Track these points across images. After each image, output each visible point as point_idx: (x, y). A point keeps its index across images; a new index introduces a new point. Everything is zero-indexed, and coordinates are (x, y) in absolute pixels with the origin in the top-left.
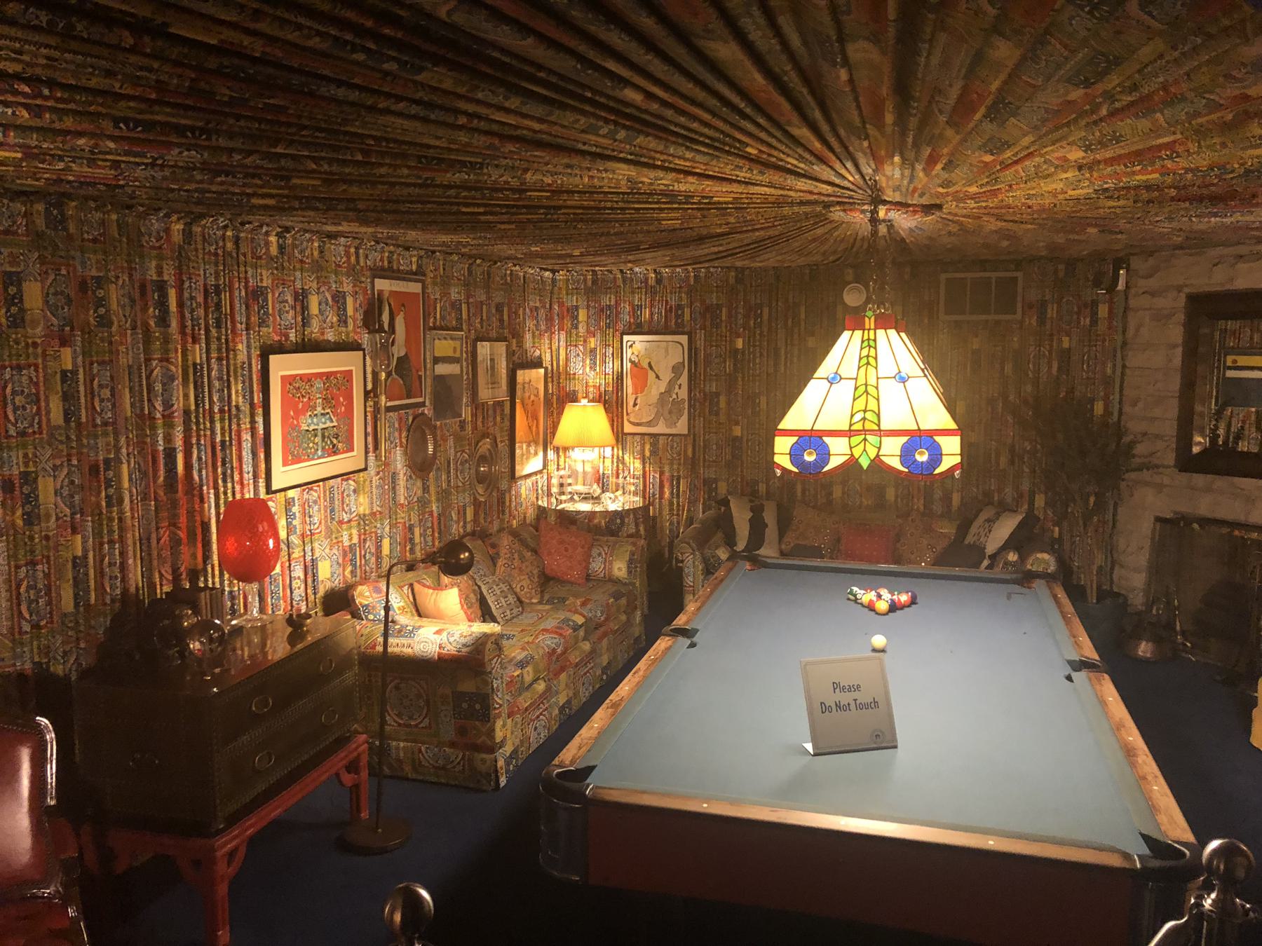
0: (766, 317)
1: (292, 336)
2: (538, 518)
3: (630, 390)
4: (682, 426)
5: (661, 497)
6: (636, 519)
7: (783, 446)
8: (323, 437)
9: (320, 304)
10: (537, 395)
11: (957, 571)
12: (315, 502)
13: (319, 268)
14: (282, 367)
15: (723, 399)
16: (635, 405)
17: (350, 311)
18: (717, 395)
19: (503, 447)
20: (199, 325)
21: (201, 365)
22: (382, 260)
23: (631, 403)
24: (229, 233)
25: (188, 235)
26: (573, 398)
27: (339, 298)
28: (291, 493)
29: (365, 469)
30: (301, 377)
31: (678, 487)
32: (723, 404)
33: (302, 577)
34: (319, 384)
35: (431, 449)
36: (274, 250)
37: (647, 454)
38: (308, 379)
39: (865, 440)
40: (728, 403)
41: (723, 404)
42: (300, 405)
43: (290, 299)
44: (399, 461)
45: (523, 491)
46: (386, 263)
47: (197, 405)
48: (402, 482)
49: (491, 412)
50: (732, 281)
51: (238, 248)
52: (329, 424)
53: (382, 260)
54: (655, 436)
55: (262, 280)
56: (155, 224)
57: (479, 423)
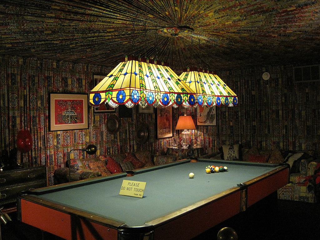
0: (239, 85)
1: (61, 89)
2: (167, 151)
3: (199, 111)
4: (214, 123)
5: (209, 147)
6: (198, 152)
7: (92, 96)
8: (71, 118)
9: (72, 81)
10: (169, 113)
11: (258, 163)
12: (69, 136)
13: (73, 72)
14: (54, 98)
15: (227, 113)
16: (200, 116)
17: (84, 83)
18: (225, 112)
19: (152, 128)
20: (26, 85)
21: (26, 95)
22: (98, 70)
23: (199, 115)
24: (39, 62)
25: (24, 63)
26: (182, 114)
27: (79, 81)
28: (59, 133)
29: (88, 129)
30: (63, 100)
31: (214, 143)
32: (227, 115)
33: (62, 157)
34: (69, 103)
35: (117, 126)
36: (55, 66)
37: (205, 132)
38: (66, 101)
39: (109, 93)
40: (229, 115)
41: (227, 115)
42: (62, 108)
43: (60, 80)
44: (104, 128)
45: (162, 143)
46: (99, 71)
47: (24, 106)
48: (105, 134)
49: (146, 117)
50: (228, 74)
51: (42, 66)
52: (73, 114)
53: (98, 70)
54: (207, 126)
55: (50, 75)
56: (14, 59)
57: (141, 120)
